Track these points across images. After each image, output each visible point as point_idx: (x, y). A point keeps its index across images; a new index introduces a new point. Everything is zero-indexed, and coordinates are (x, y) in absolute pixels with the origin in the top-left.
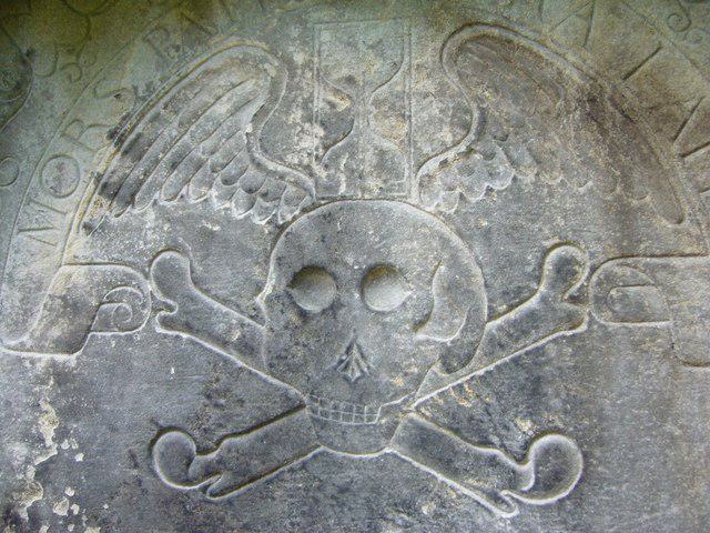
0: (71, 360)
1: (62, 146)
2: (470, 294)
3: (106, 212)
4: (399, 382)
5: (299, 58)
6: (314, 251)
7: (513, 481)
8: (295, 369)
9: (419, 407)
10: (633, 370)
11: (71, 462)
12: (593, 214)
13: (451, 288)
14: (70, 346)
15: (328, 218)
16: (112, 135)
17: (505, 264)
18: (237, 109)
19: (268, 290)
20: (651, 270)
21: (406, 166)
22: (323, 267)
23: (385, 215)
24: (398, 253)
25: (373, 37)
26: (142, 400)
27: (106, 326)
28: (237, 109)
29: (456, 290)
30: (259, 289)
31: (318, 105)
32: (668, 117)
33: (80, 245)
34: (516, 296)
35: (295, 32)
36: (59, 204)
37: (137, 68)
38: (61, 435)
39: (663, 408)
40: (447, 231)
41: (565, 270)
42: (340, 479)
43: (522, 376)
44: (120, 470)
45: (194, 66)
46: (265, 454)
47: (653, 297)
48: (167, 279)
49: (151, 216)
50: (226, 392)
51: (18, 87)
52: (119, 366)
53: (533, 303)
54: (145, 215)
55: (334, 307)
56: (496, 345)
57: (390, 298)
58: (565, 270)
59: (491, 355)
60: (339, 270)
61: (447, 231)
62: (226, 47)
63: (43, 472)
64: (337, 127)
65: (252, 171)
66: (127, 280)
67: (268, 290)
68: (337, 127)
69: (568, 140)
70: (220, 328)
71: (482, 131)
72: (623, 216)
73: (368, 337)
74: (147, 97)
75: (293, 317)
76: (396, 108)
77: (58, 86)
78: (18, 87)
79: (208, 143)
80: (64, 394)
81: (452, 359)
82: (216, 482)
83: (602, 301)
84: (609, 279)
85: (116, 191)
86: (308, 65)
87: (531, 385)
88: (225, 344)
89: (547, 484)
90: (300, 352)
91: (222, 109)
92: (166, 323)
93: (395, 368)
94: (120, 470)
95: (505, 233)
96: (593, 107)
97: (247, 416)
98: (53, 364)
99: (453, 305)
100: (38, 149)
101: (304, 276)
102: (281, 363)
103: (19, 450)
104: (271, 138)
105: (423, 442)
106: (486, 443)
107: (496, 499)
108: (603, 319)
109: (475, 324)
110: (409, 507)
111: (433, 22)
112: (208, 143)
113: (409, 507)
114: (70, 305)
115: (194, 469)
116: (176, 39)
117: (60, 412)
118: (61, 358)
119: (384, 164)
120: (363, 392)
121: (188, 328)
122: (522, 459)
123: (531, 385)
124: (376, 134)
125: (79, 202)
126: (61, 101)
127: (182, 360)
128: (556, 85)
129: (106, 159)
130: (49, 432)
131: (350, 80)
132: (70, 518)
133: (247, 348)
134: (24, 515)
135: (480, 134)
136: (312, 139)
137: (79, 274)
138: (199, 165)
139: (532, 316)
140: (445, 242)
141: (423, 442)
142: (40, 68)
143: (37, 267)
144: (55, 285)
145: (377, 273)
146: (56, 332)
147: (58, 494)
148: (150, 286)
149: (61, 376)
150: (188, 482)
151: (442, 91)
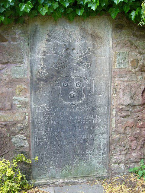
0: (44, 57)
1: (42, 35)
2: (81, 51)
3: (47, 42)
4: (76, 59)
5: (66, 29)
6: (68, 47)
7: (85, 67)
8: (67, 58)
9: (77, 61)
10: (94, 58)
11: (45, 67)
12: (91, 45)
13: (80, 51)
14: (44, 56)
15: (69, 44)
16: (47, 35)
17: (84, 49)
18: (60, 33)
19: (64, 50)
20: (96, 49)
21: (76, 40)
22: (69, 48)
23: (74, 44)
24: (76, 47)
25: (73, 27)
26: (52, 61)
27: (48, 54)
28: (60, 33)
29: (80, 51)
30: (63, 50)
31: (68, 33)
32: (97, 37)
33: (45, 46)
34: (85, 51)
35: (66, 26)
36: (42, 41)
37: (49, 28)
38: (44, 64)
39: (96, 61)
40: (79, 46)
41: (89, 49)
42: (71, 67)
43: (86, 58)
44: (50, 67)
45: (56, 28)
46: (64, 65)
47: (96, 52)
48: (54, 49)
49: (52, 43)
50: (60, 60)
51: (36, 28)
52: (50, 57)
53: (86, 52)
54: (51, 43)
55: (70, 52)
56: (84, 56)
57: (75, 51)
58: (89, 49)
59: (83, 56)
60: (70, 49)
61: (79, 46)
62: (59, 27)
63: (42, 68)
64: (70, 35)
65: (62, 39)
66: (50, 49)
67: (64, 50)
68: (70, 35)
69: (89, 38)
70: (59, 54)
71: (83, 37)
72: (94, 45)
73: (73, 55)
74: (51, 31)
75: (66, 53)
76: (75, 34)
77: (41, 29)
78: (36, 28)
79: (57, 36)
80: (44, 60)
81: (80, 57)
82: (60, 68)
83: (92, 52)
84: (92, 50)
85: (48, 40)
86: (67, 29)
87: (86, 59)
88: (60, 55)
89: (87, 67)
90: (67, 56)
91: (59, 33)
92: (54, 53)
93: (75, 57)
94: (50, 67)
95: (84, 46)
96: (92, 35)
97: (62, 62)
98: (43, 57)
99: (80, 52)
100: (39, 36)
101: (67, 49)
102: (65, 57)
103: (39, 66)
104: (64, 36)
105: (78, 64)
106: (83, 64)
107: (83, 68)
108: (92, 53)
109: (82, 54)
110: (76, 69)
111: (78, 26)
112: (57, 36)
113: (76, 69)
114: (44, 52)
115: (57, 67)
116: (54, 25)
117: (44, 62)
118: (43, 57)
119: (74, 39)
120: (73, 59)
121: (56, 54)
122: (85, 65)
123: (86, 59)
124: (73, 36)
125: (44, 41)
126: (41, 31)
127: (56, 57)
128: (89, 33)
129: (47, 37)
130: (42, 64)
131: (71, 31)
132: (45, 72)
133: (62, 56)
134: (40, 72)
135: (82, 37)
136: (67, 37)
137: (45, 49)
138: (57, 38)
139: (86, 53)
140: (79, 47)
141: (78, 64)
142: (39, 27)
143: (40, 48)
144: (42, 50)
145: (74, 49)
146: (42, 54)
147: (44, 70)
148: (52, 50)
149: (43, 59)
150: (57, 68)
151: (79, 33)
